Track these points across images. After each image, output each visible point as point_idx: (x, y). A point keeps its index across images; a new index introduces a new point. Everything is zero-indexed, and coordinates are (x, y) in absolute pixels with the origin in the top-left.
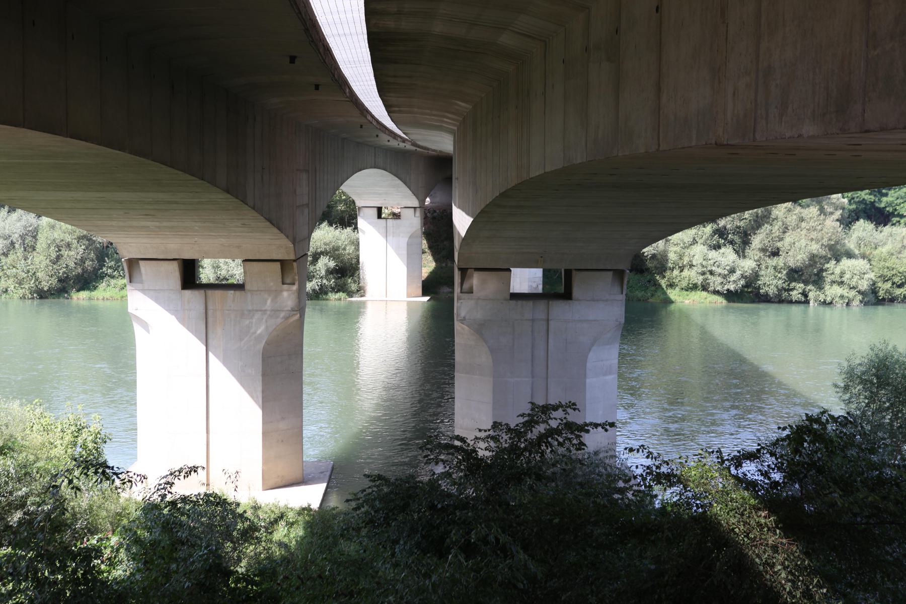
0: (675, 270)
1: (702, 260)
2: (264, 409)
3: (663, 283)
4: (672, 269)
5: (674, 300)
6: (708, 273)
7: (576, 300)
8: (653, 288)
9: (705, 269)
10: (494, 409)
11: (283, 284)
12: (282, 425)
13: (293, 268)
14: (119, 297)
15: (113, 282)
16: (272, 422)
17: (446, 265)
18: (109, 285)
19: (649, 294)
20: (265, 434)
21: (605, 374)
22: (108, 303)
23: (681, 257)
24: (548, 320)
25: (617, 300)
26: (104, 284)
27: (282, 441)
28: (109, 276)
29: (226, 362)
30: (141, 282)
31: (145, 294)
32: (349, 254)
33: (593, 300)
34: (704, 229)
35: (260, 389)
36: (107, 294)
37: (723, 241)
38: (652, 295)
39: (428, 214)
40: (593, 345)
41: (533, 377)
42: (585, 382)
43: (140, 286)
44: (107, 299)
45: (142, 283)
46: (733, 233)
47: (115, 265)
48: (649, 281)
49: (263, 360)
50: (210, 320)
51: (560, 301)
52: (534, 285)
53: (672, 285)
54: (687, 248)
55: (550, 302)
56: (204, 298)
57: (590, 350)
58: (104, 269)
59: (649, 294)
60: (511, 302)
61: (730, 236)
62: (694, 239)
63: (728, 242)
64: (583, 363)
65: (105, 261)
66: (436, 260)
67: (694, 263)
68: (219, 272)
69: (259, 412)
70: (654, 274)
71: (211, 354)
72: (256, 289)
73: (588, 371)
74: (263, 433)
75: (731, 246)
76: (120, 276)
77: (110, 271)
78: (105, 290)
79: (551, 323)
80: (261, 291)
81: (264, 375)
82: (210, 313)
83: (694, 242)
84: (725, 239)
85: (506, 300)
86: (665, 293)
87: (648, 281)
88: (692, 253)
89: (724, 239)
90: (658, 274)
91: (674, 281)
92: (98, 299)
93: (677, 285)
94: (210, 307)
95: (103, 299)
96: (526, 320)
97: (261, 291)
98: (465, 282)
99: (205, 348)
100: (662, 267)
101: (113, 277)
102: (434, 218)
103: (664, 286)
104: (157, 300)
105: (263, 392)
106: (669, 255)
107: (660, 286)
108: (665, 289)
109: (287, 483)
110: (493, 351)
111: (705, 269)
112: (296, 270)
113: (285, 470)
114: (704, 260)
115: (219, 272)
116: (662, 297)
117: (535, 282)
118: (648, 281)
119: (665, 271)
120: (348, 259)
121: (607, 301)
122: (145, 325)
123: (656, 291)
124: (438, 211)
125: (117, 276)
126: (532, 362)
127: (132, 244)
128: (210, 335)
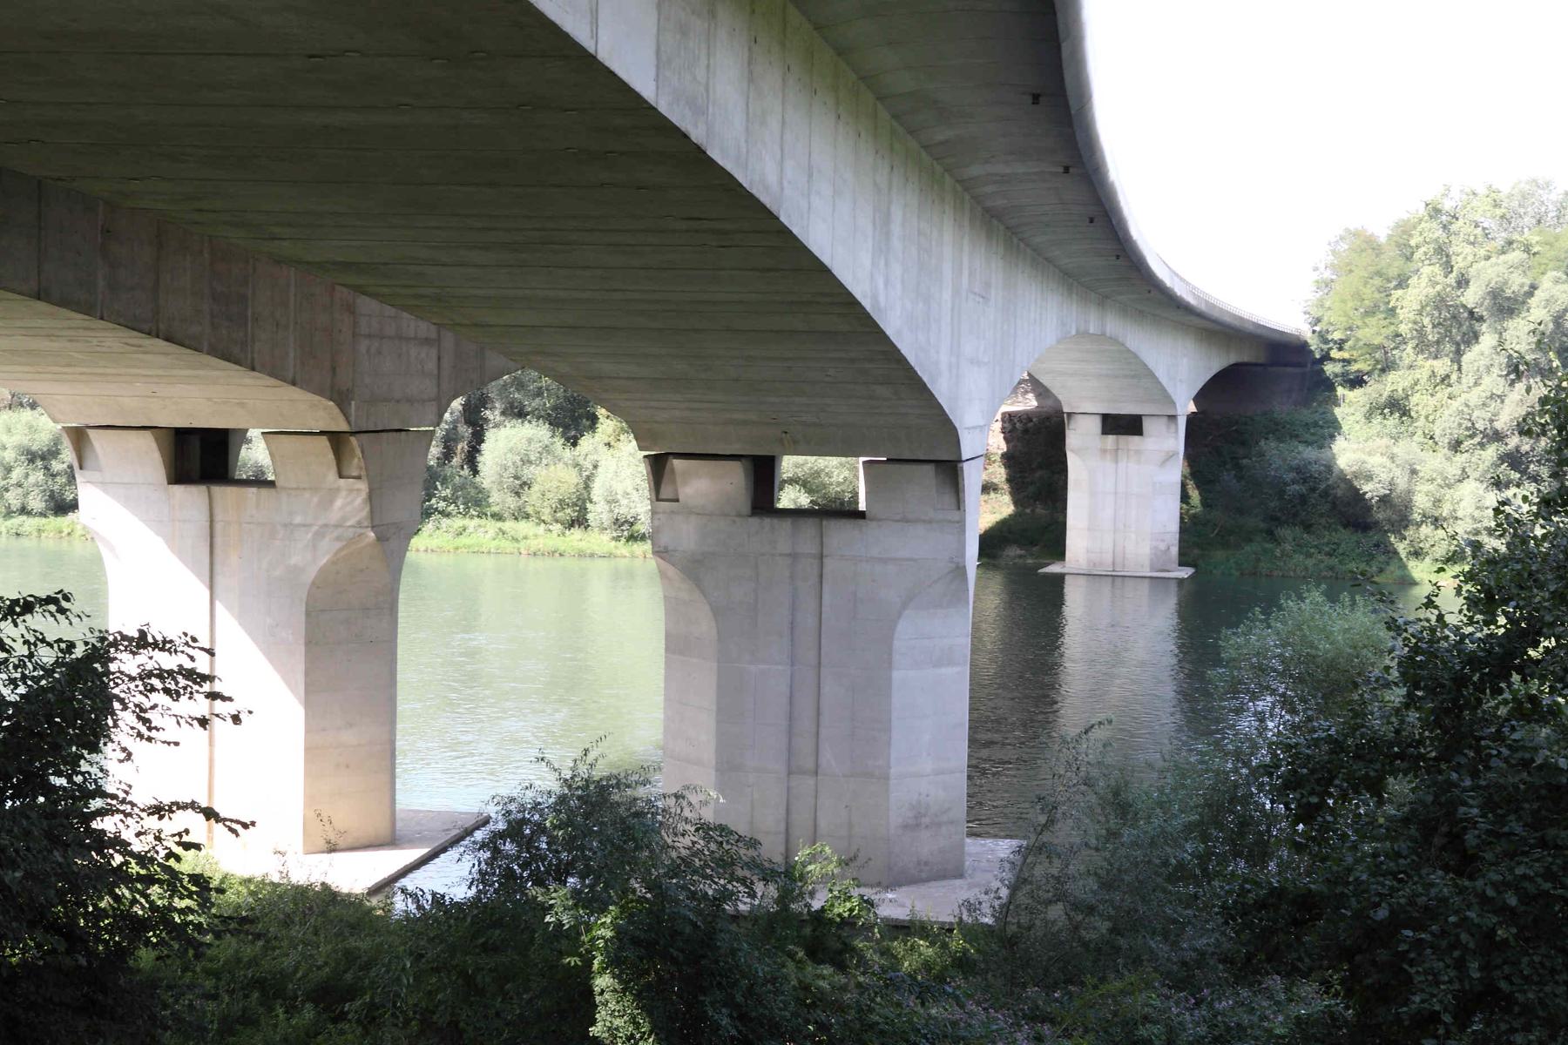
0: (1424, 526)
1: (1474, 508)
2: (308, 704)
3: (1402, 548)
4: (1419, 525)
5: (1418, 580)
6: (1484, 532)
7: (871, 520)
8: (1383, 558)
9: (1479, 525)
10: (718, 722)
11: (341, 476)
12: (349, 737)
13: (353, 450)
14: (451, 547)
15: (445, 522)
16: (324, 730)
17: (1033, 511)
18: (438, 528)
19: (1374, 568)
20: (311, 751)
21: (938, 664)
22: (434, 557)
23: (1437, 502)
24: (821, 557)
25: (950, 521)
26: (430, 526)
27: (347, 766)
28: (440, 513)
29: (243, 617)
30: (100, 470)
31: (105, 491)
32: (839, 484)
33: (905, 520)
34: (1482, 452)
35: (301, 667)
36: (434, 543)
37: (1518, 475)
38: (1381, 571)
39: (1018, 425)
40: (904, 606)
41: (792, 665)
42: (889, 679)
43: (96, 476)
44: (432, 551)
45: (100, 471)
46: (1537, 461)
47: (453, 495)
48: (1377, 545)
49: (308, 614)
50: (218, 540)
51: (844, 520)
52: (1162, 546)
53: (1417, 554)
54: (1449, 486)
55: (825, 523)
56: (207, 501)
57: (900, 615)
58: (434, 501)
59: (1374, 568)
60: (750, 519)
61: (1532, 466)
62: (1463, 470)
63: (1528, 479)
64: (886, 639)
65: (436, 489)
66: (1016, 503)
67: (1460, 514)
68: (616, 511)
69: (300, 711)
70: (1386, 532)
71: (219, 605)
72: (295, 486)
73: (896, 657)
74: (307, 750)
75: (1533, 484)
76: (460, 513)
77: (442, 505)
78: (431, 535)
79: (825, 560)
80: (304, 489)
81: (309, 643)
82: (218, 527)
83: (1464, 476)
84: (1523, 472)
85: (739, 515)
86: (1404, 567)
87: (1375, 546)
88: (1457, 496)
89: (1520, 472)
90: (1393, 532)
91: (1421, 545)
92: (418, 550)
93: (1427, 553)
94: (219, 517)
95: (426, 551)
96: (781, 555)
97: (304, 489)
98: (663, 486)
99: (207, 593)
100: (1402, 520)
101: (448, 515)
102: (1026, 431)
103: (1403, 555)
104: (127, 502)
105: (307, 674)
106: (1415, 498)
107: (1396, 553)
108: (1405, 559)
109: (357, 845)
110: (717, 612)
111: (1479, 525)
112: (358, 452)
113: (348, 817)
114: (1478, 508)
115: (616, 511)
116: (1398, 573)
117: (1163, 541)
118: (1375, 546)
119: (1406, 527)
120: (836, 492)
121: (930, 522)
122: (112, 549)
123: (1388, 564)
124: (1034, 420)
125: (454, 513)
126: (792, 633)
127: (59, 397)
128: (218, 568)
